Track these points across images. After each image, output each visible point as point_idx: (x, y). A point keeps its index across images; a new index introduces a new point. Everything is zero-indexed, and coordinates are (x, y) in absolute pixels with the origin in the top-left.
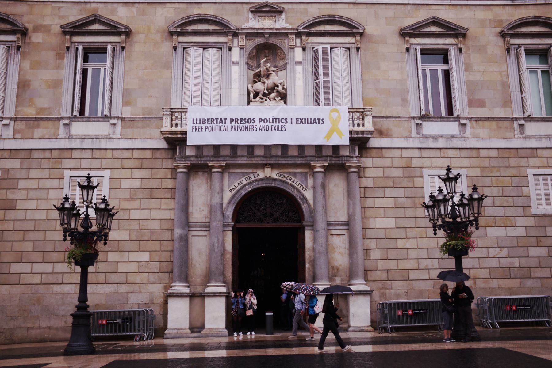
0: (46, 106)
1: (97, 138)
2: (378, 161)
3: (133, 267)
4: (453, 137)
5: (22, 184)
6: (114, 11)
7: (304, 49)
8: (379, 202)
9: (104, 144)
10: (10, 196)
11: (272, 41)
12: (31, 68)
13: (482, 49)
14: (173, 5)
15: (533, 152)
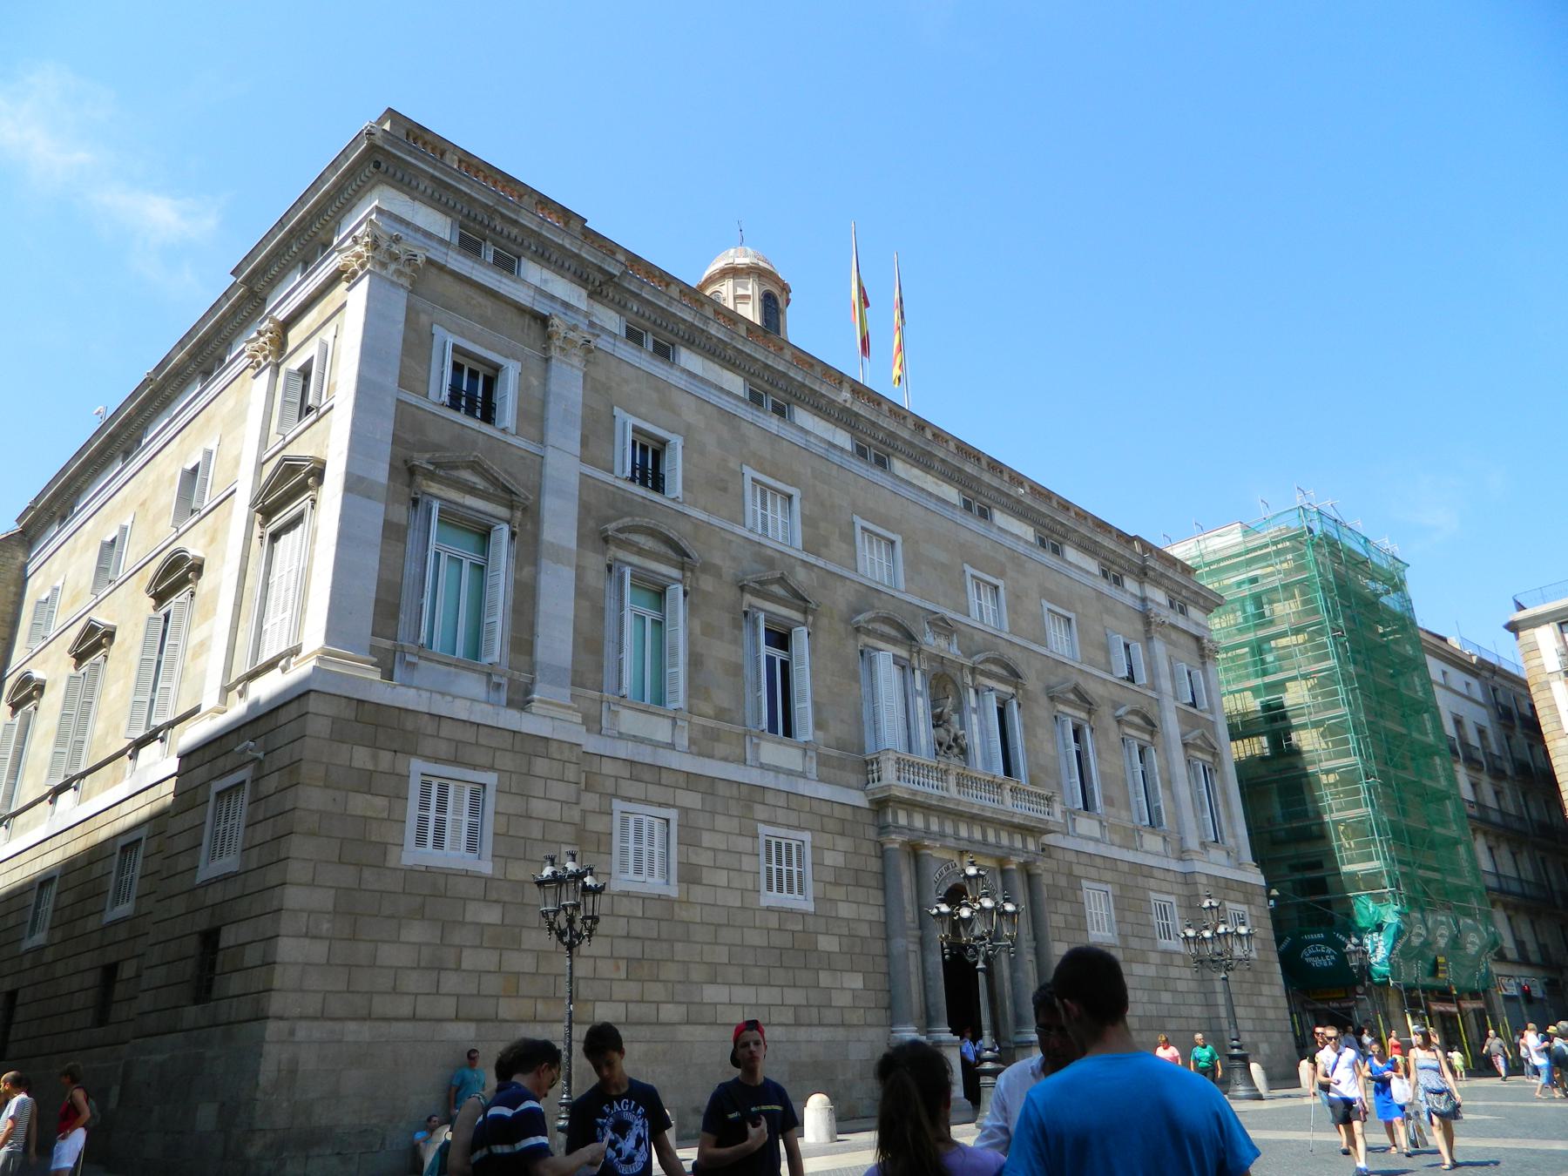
0: (726, 705)
1: (790, 773)
4: (1096, 840)
5: (707, 839)
7: (977, 692)
10: (694, 859)
12: (703, 634)
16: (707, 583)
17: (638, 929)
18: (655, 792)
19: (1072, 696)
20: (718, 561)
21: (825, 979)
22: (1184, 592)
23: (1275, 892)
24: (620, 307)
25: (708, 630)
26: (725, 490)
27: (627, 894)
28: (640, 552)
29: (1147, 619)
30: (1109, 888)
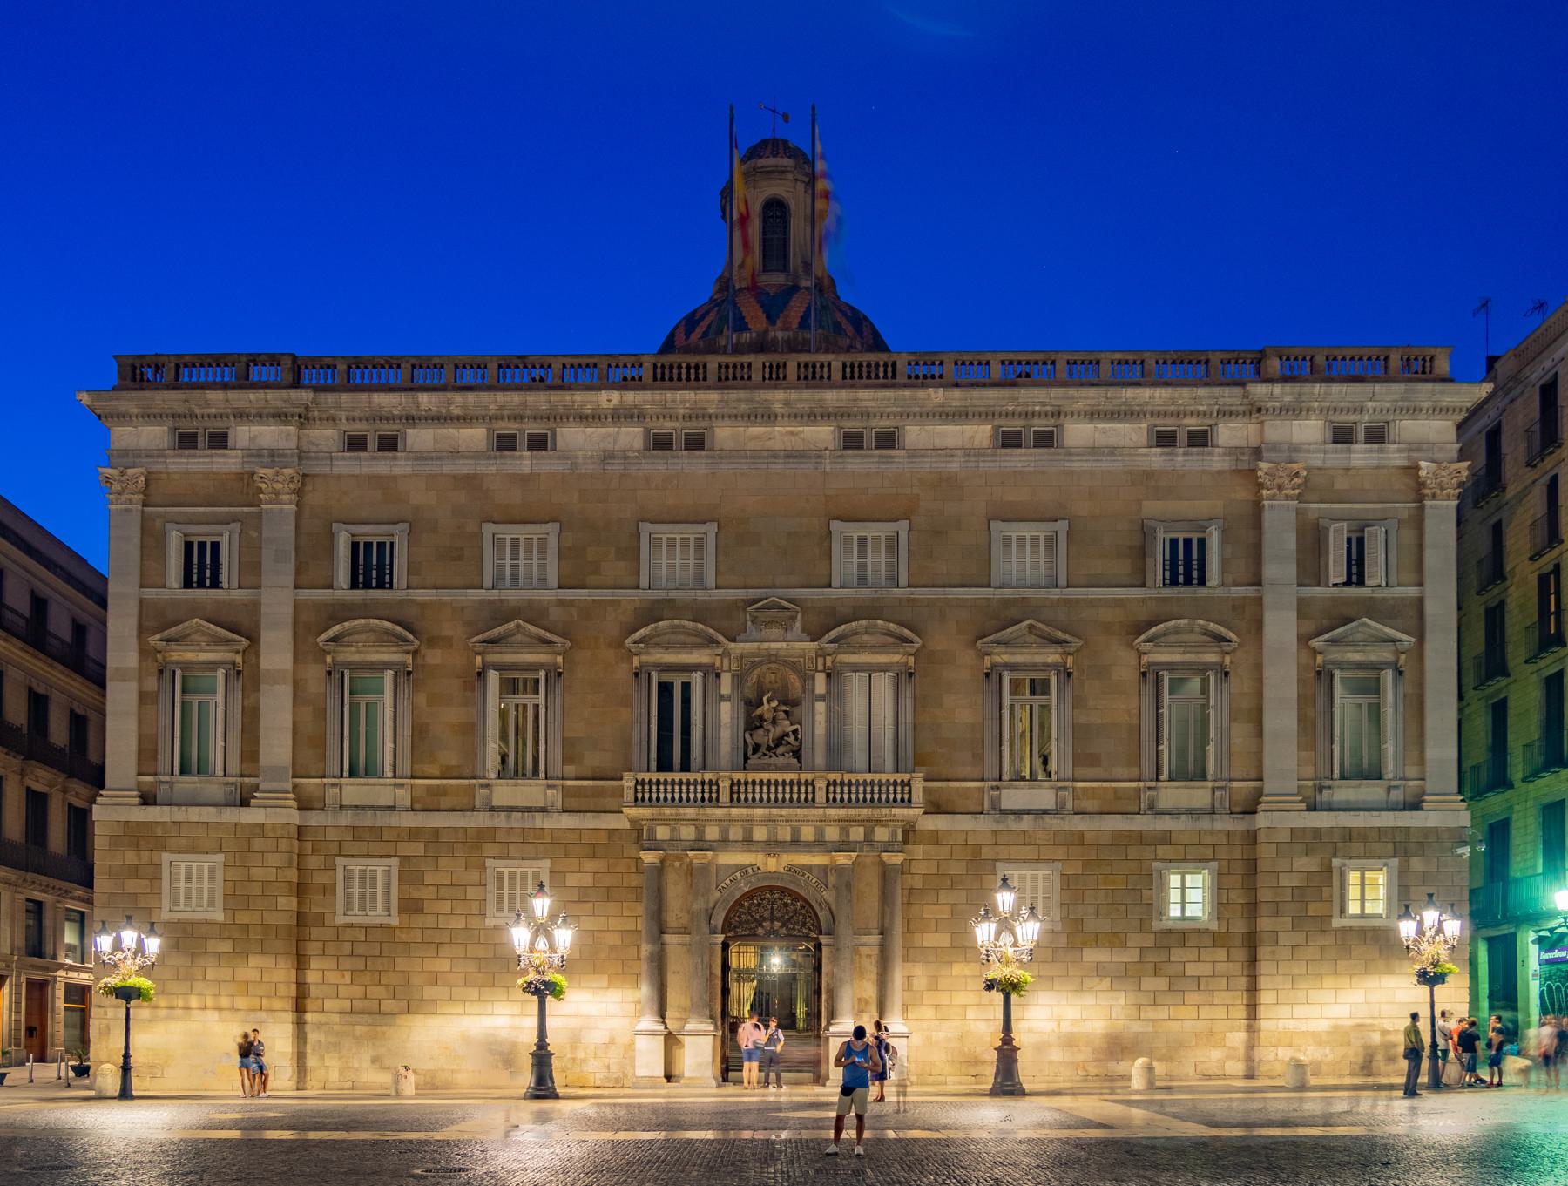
0: (454, 763)
1: (529, 810)
2: (930, 848)
4: (1045, 812)
5: (429, 879)
7: (828, 675)
8: (931, 911)
10: (415, 895)
15: (1166, 838)
16: (434, 657)
17: (361, 949)
18: (375, 847)
26: (460, 558)
27: (352, 926)
30: (1059, 865)
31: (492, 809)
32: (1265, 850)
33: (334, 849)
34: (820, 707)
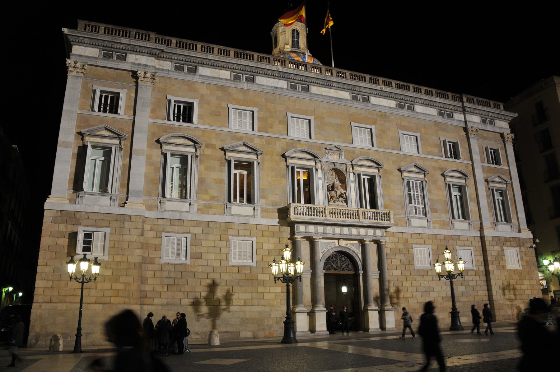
0: (216, 195)
1: (247, 216)
3: (272, 296)
4: (425, 227)
5: (204, 243)
6: (252, 140)
7: (354, 174)
9: (252, 221)
10: (197, 250)
11: (338, 167)
13: (435, 182)
14: (285, 140)
15: (458, 238)
16: (208, 152)
17: (172, 275)
18: (181, 229)
19: (414, 169)
20: (214, 142)
21: (260, 289)
22: (490, 114)
23: (537, 241)
24: (171, 59)
25: (207, 169)
26: (219, 115)
28: (176, 145)
29: (465, 129)
30: (430, 247)
31: (232, 215)
32: (487, 243)
33: (161, 228)
34: (352, 185)
